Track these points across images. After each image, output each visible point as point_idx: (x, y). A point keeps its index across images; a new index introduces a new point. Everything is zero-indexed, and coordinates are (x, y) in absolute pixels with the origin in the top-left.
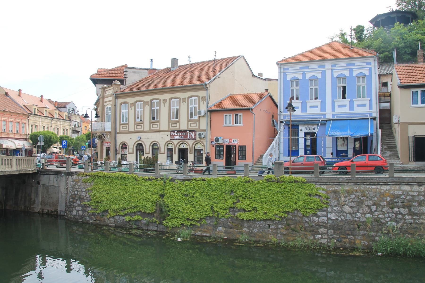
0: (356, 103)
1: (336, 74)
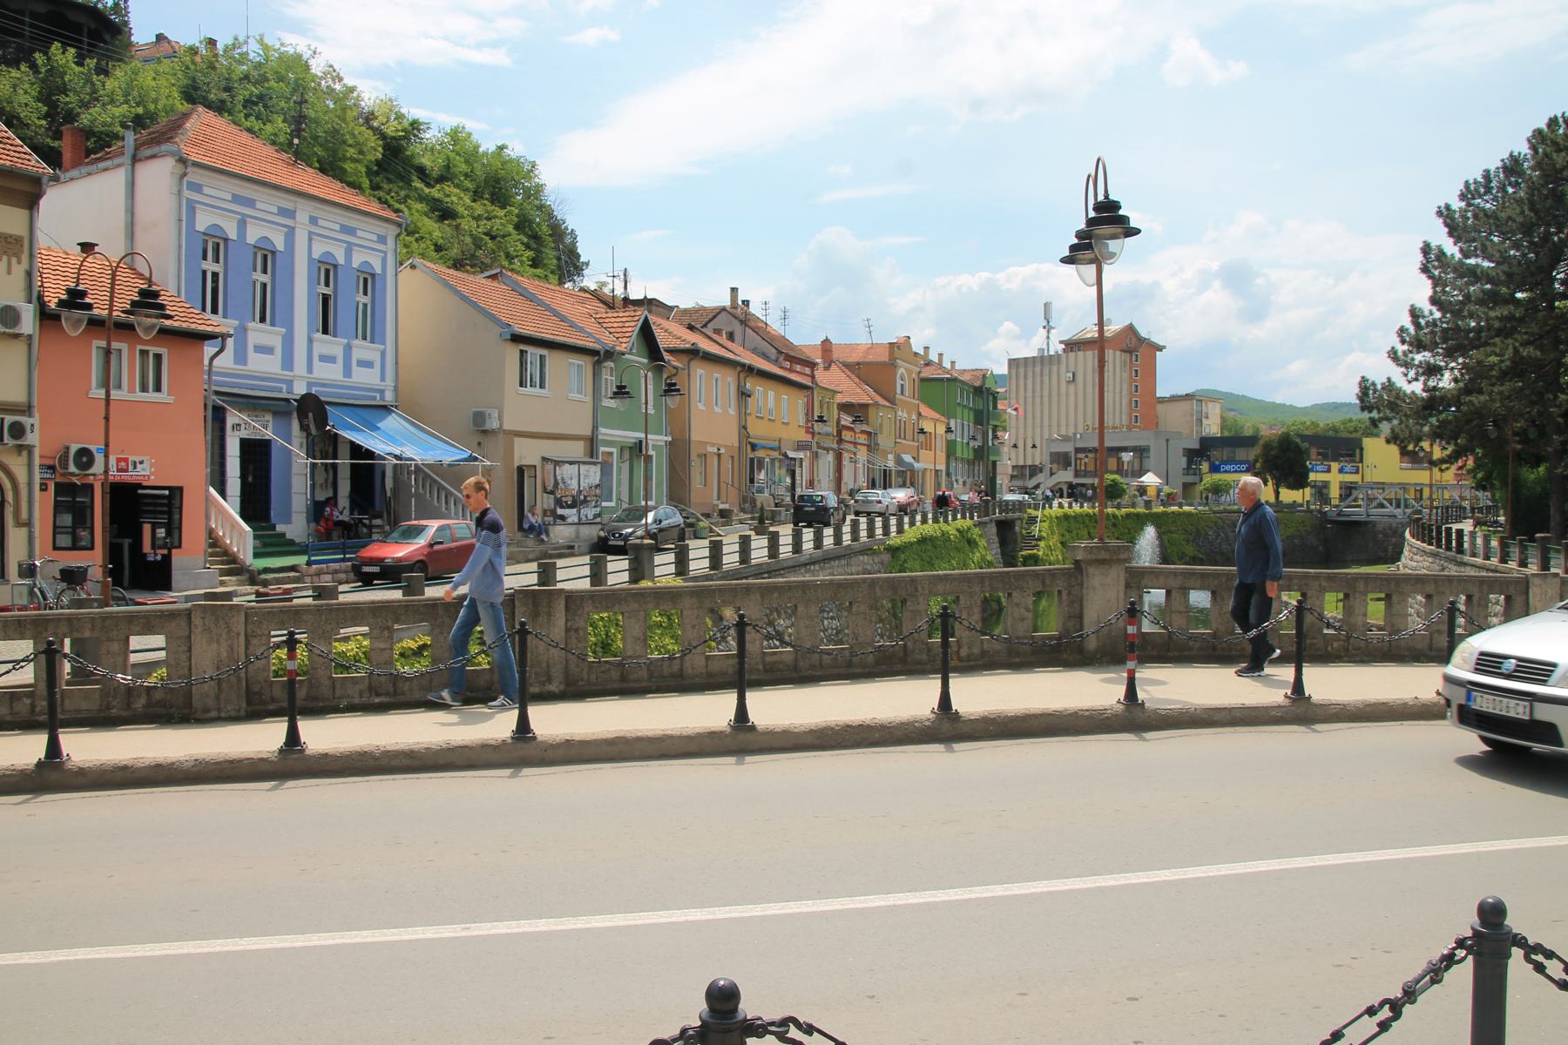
0: (357, 354)
1: (319, 250)
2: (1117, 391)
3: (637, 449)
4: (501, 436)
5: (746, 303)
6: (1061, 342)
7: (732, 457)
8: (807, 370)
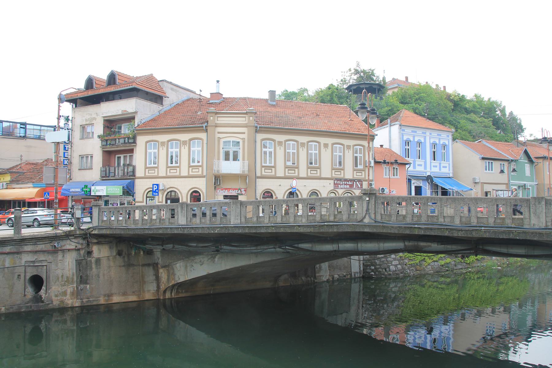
0: (442, 165)
4: (480, 184)
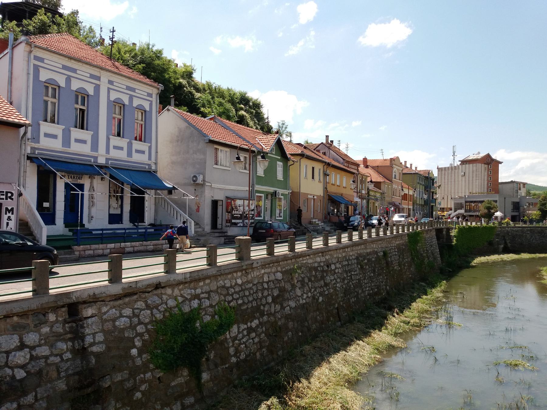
1: (114, 96)
2: (483, 179)
3: (274, 194)
5: (332, 142)
6: (459, 161)
7: (320, 200)
8: (356, 167)
